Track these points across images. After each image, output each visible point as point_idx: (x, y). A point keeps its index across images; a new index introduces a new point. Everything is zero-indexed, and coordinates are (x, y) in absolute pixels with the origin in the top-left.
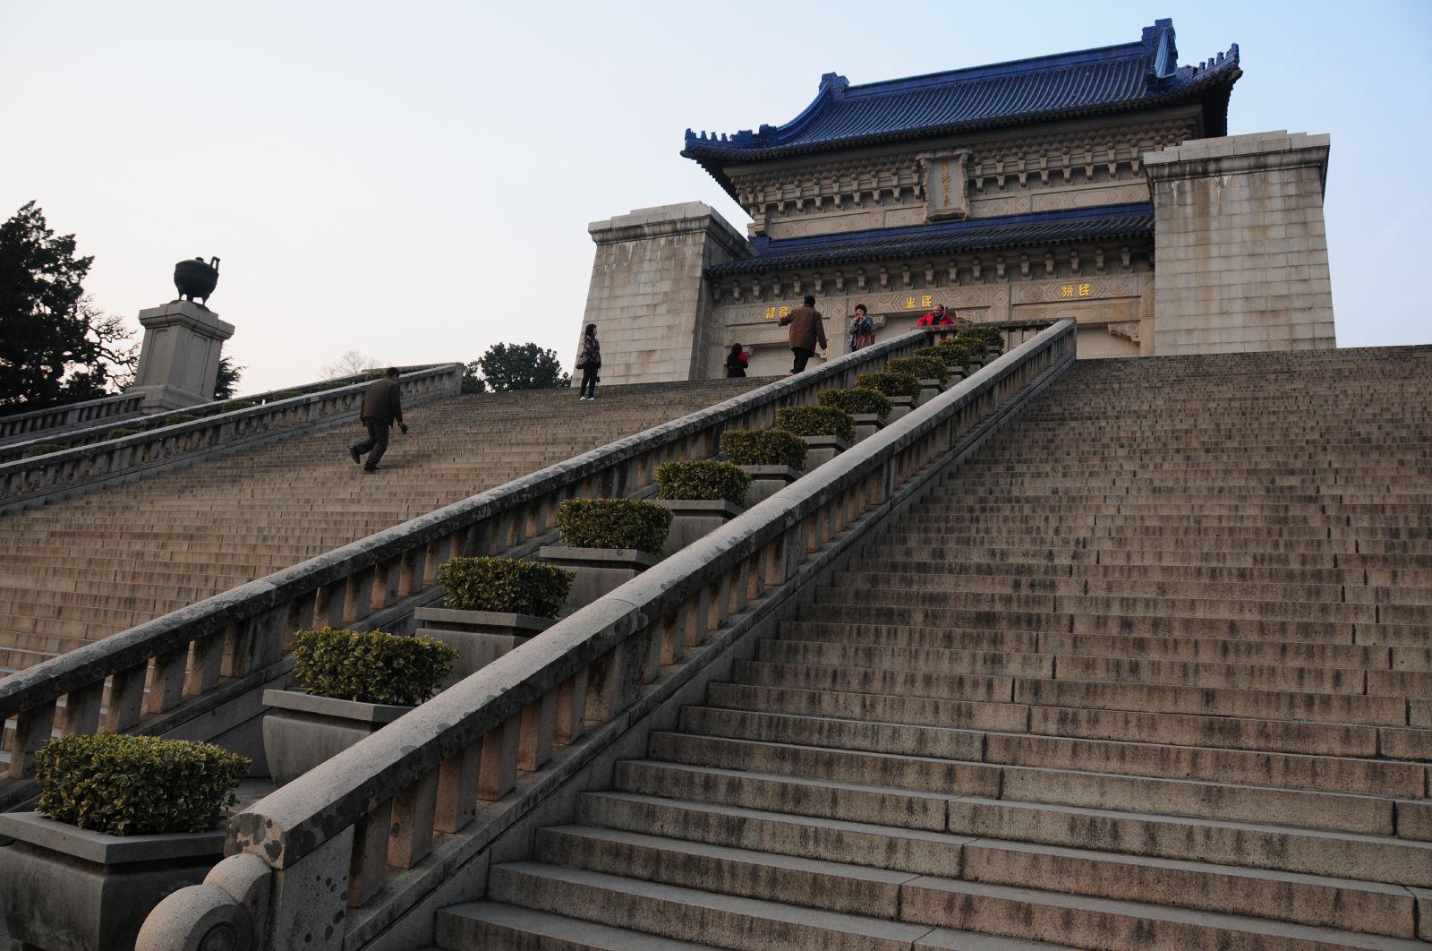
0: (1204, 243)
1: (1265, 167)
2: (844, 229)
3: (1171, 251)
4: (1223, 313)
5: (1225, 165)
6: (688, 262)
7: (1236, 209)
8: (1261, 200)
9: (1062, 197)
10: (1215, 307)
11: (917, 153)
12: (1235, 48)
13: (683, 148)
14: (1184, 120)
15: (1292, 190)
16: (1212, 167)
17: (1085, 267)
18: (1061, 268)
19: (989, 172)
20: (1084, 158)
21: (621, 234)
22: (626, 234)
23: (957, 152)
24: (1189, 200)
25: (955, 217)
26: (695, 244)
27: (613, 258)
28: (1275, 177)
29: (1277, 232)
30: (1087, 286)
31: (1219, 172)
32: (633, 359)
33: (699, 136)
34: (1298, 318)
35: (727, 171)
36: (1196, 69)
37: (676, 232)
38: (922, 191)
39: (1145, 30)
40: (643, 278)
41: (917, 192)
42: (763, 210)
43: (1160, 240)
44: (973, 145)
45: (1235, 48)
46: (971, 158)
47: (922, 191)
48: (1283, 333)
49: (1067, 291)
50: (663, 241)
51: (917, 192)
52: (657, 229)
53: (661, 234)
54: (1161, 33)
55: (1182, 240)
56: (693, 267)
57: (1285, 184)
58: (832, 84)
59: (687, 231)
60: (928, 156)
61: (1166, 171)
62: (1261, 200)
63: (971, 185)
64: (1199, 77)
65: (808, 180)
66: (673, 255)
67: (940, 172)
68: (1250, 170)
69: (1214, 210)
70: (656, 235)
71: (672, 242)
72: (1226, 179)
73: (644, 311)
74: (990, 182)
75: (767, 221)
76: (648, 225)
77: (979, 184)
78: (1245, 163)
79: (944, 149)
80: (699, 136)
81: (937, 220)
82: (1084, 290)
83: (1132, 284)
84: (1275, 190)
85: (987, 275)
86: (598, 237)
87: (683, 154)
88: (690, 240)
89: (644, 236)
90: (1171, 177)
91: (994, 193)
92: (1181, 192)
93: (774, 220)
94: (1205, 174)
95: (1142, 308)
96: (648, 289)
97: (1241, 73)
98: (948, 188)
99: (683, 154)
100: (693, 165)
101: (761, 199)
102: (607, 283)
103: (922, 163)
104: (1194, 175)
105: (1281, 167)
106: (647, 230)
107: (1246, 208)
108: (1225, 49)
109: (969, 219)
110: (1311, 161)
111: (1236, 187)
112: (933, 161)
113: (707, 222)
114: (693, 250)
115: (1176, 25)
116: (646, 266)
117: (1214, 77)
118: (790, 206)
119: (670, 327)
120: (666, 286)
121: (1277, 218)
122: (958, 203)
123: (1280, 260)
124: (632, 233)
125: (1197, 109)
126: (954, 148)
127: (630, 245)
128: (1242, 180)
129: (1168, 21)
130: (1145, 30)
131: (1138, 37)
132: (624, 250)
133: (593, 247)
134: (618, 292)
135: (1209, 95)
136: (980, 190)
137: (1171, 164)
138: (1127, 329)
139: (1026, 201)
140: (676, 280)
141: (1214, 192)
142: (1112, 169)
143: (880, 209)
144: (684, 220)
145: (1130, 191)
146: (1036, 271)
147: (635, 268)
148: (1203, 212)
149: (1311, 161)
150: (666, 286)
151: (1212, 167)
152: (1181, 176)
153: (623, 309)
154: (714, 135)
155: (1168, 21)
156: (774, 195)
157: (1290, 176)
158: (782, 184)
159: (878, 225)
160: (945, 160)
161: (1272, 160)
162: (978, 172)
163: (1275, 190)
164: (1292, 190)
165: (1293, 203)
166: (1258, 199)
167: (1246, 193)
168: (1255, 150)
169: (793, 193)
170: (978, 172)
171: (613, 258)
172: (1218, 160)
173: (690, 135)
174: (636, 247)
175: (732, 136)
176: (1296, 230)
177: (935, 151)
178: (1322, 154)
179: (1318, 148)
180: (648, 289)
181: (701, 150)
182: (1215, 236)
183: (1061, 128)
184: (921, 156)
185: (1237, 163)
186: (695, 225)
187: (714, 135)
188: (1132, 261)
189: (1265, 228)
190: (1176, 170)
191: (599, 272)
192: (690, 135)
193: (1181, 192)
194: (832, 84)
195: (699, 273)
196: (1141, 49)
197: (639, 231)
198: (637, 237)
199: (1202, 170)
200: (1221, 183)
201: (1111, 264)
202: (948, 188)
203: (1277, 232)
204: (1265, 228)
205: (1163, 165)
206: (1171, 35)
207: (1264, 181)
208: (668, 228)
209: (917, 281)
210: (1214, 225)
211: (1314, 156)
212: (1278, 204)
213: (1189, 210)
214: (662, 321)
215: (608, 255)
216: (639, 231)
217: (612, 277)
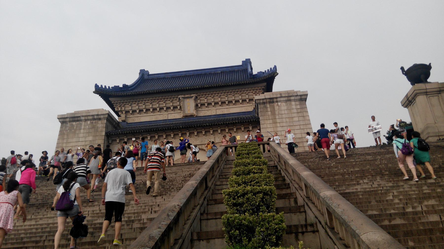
0: (275, 123)
1: (290, 100)
2: (154, 120)
3: (266, 125)
5: (279, 99)
6: (99, 130)
7: (283, 112)
8: (290, 110)
9: (226, 110)
11: (178, 95)
12: (275, 67)
13: (94, 90)
14: (261, 87)
15: (298, 107)
16: (275, 100)
20: (231, 98)
21: (71, 120)
22: (74, 119)
23: (192, 95)
24: (269, 110)
25: (192, 116)
26: (102, 123)
27: (68, 128)
28: (293, 103)
29: (296, 119)
30: (239, 136)
31: (277, 102)
33: (100, 86)
35: (110, 99)
36: (263, 73)
37: (94, 119)
38: (180, 107)
39: (243, 62)
40: (81, 135)
41: (179, 107)
42: (124, 113)
43: (261, 122)
44: (197, 93)
45: (275, 67)
46: (196, 97)
50: (89, 122)
51: (179, 107)
52: (86, 118)
53: (88, 120)
54: (247, 62)
55: (268, 122)
56: (102, 131)
57: (296, 105)
58: (143, 73)
59: (100, 119)
60: (182, 96)
61: (262, 101)
62: (290, 110)
63: (197, 105)
64: (265, 75)
65: (141, 103)
66: (93, 127)
68: (286, 101)
69: (277, 113)
70: (86, 120)
71: (93, 122)
72: (279, 103)
74: (203, 105)
75: (126, 117)
76: (83, 116)
77: (199, 106)
78: (284, 99)
79: (188, 94)
80: (100, 86)
81: (186, 117)
84: (294, 107)
86: (61, 120)
87: (94, 92)
88: (100, 122)
89: (81, 120)
90: (264, 103)
91: (204, 108)
93: (128, 116)
94: (273, 102)
96: (83, 139)
97: (278, 74)
98: (189, 106)
99: (94, 92)
100: (97, 96)
101: (123, 109)
102: (65, 137)
103: (181, 98)
104: (270, 102)
105: (295, 100)
106: (83, 118)
108: (272, 67)
109: (196, 116)
110: (302, 98)
111: (282, 107)
112: (184, 98)
113: (107, 116)
114: (101, 125)
115: (251, 60)
116: (82, 131)
117: (270, 74)
118: (134, 111)
121: (295, 115)
123: (298, 127)
124: (76, 119)
125: (265, 84)
126: (191, 94)
128: (284, 104)
129: (249, 59)
130: (243, 62)
131: (240, 64)
132: (73, 126)
133: (59, 124)
134: (70, 140)
135: (267, 80)
136: (200, 108)
137: (263, 99)
139: (215, 111)
141: (276, 108)
142: (241, 101)
143: (166, 113)
144: (98, 115)
145: (249, 108)
147: (77, 132)
148: (273, 113)
149: (302, 98)
151: (275, 100)
154: (105, 86)
155: (249, 59)
156: (128, 108)
157: (298, 103)
158: (131, 104)
161: (292, 98)
162: (199, 102)
163: (294, 107)
164: (298, 107)
165: (299, 111)
166: (289, 109)
167: (285, 108)
168: (287, 95)
169: (135, 107)
170: (199, 102)
171: (68, 128)
172: (276, 98)
173: (96, 86)
175: (112, 87)
176: (301, 118)
177: (184, 95)
178: (306, 97)
179: (305, 95)
180: (83, 139)
181: (103, 92)
182: (278, 121)
184: (180, 96)
185: (282, 99)
186: (102, 117)
187: (105, 86)
188: (252, 128)
189: (292, 118)
190: (265, 101)
191: (62, 133)
192: (96, 86)
193: (266, 108)
194: (143, 73)
195: (104, 134)
196: (241, 67)
197: (79, 119)
198: (78, 121)
199: (272, 101)
200: (278, 105)
202: (189, 106)
203: (296, 119)
204: (292, 118)
205: (260, 99)
206: (250, 63)
207: (291, 104)
208: (91, 118)
210: (277, 117)
211: (303, 97)
212: (295, 111)
213: (269, 113)
215: (66, 127)
216: (79, 119)
217: (67, 135)
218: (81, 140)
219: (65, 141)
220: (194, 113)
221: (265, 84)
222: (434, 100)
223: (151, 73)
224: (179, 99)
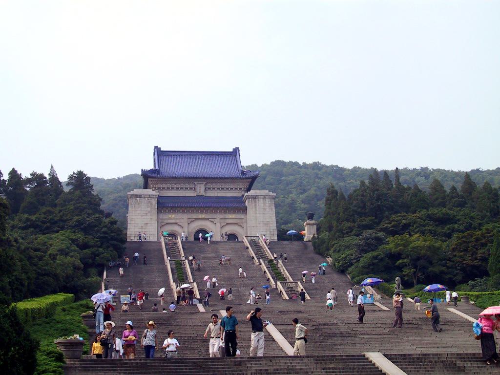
0: (256, 210)
4: (259, 224)
5: (259, 197)
10: (258, 223)
17: (234, 212)
18: (230, 212)
19: (209, 187)
25: (202, 196)
28: (267, 200)
31: (258, 198)
32: (143, 225)
34: (271, 225)
37: (150, 197)
47: (195, 188)
48: (268, 228)
49: (230, 216)
54: (236, 151)
57: (269, 201)
67: (199, 185)
73: (144, 215)
77: (207, 189)
79: (200, 181)
82: (234, 216)
83: (242, 216)
84: (267, 202)
85: (216, 212)
91: (209, 191)
92: (252, 201)
94: (256, 198)
95: (244, 221)
98: (201, 189)
106: (143, 196)
107: (262, 205)
115: (240, 149)
119: (151, 219)
120: (149, 209)
121: (267, 207)
122: (202, 192)
123: (268, 215)
127: (138, 199)
128: (262, 200)
131: (232, 151)
138: (241, 224)
140: (151, 208)
141: (257, 201)
146: (225, 212)
148: (256, 205)
150: (149, 209)
152: (252, 198)
153: (139, 213)
157: (269, 200)
159: (184, 196)
160: (200, 183)
161: (267, 197)
163: (267, 202)
166: (264, 204)
173: (142, 170)
174: (140, 200)
177: (198, 181)
183: (225, 180)
185: (262, 197)
192: (142, 170)
193: (252, 201)
199: (255, 197)
201: (239, 211)
202: (201, 189)
206: (239, 150)
209: (202, 212)
212: (267, 205)
214: (150, 217)
218: (143, 209)
219: (133, 209)
220: (204, 194)
221: (251, 180)
222: (311, 227)
223: (162, 149)
224: (195, 183)
